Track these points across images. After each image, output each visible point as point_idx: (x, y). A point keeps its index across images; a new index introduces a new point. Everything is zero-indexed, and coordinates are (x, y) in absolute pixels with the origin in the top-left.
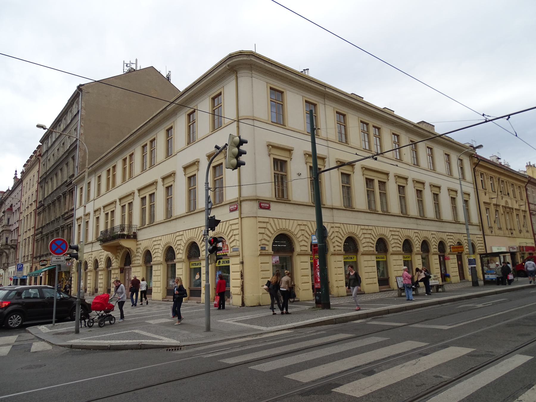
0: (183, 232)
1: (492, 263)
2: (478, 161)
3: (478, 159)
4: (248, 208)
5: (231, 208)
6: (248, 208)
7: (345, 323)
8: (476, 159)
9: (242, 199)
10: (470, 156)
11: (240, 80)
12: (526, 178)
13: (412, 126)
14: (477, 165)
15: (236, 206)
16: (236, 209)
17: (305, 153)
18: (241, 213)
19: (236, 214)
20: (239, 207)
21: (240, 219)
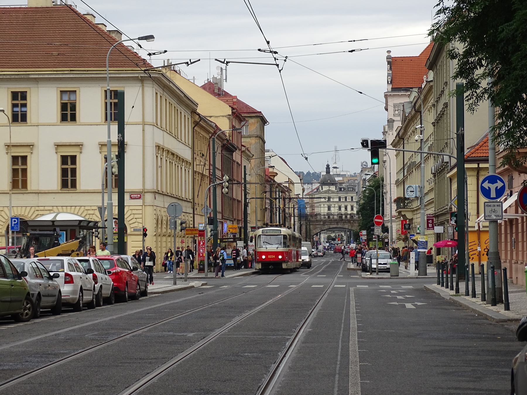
0: (53, 208)
1: (229, 249)
2: (200, 119)
3: (200, 116)
4: (149, 197)
5: (132, 196)
6: (149, 197)
7: (26, 323)
8: (198, 116)
9: (146, 191)
10: (192, 112)
11: (146, 89)
12: (213, 127)
13: (183, 95)
14: (196, 124)
15: (139, 196)
16: (140, 198)
17: (157, 145)
18: (144, 202)
19: (139, 202)
20: (142, 196)
21: (143, 206)
